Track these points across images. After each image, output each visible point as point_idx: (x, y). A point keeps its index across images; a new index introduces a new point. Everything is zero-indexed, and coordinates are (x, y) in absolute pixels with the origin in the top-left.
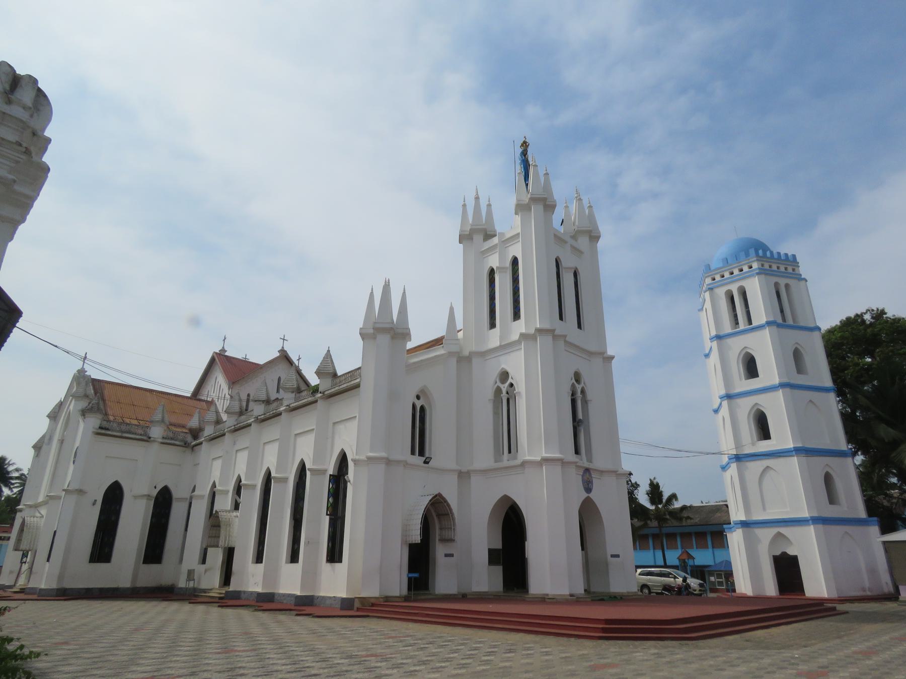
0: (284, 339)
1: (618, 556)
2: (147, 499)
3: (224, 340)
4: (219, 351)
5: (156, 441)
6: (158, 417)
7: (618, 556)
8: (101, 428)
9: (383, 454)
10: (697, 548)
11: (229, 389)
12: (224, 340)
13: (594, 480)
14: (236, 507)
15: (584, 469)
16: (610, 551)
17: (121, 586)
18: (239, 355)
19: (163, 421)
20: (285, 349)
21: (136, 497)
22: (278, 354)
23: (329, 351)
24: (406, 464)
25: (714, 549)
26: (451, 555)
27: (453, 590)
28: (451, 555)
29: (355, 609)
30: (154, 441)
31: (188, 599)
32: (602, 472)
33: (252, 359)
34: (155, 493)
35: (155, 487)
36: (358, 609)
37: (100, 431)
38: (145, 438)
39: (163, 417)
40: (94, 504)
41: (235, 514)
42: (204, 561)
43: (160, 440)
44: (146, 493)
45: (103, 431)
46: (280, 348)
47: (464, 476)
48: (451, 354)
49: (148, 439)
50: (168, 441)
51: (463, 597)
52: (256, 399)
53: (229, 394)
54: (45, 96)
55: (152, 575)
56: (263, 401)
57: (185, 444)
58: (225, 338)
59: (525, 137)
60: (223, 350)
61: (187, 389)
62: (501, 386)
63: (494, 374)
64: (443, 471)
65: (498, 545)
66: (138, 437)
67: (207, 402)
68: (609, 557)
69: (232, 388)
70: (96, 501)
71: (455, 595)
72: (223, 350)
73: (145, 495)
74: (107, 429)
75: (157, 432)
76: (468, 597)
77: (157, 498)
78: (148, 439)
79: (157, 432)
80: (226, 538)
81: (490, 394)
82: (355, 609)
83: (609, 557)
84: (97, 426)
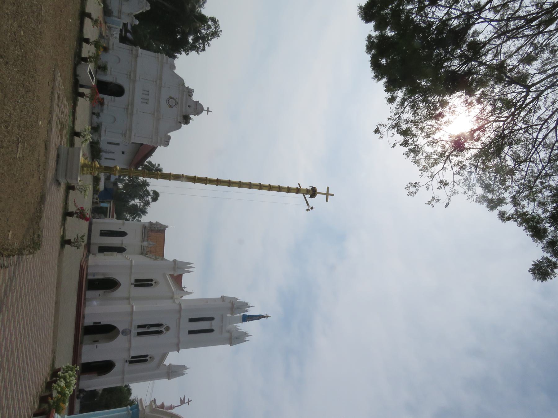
6: (151, 243)
8: (145, 227)
9: (133, 264)
13: (127, 336)
19: (149, 244)
21: (122, 241)
27: (87, 297)
34: (124, 246)
35: (126, 246)
37: (144, 227)
40: (120, 229)
43: (143, 245)
44: (124, 243)
48: (173, 293)
49: (143, 241)
55: (95, 249)
59: (270, 316)
65: (102, 324)
70: (121, 229)
74: (145, 229)
75: (145, 244)
77: (122, 248)
79: (145, 244)
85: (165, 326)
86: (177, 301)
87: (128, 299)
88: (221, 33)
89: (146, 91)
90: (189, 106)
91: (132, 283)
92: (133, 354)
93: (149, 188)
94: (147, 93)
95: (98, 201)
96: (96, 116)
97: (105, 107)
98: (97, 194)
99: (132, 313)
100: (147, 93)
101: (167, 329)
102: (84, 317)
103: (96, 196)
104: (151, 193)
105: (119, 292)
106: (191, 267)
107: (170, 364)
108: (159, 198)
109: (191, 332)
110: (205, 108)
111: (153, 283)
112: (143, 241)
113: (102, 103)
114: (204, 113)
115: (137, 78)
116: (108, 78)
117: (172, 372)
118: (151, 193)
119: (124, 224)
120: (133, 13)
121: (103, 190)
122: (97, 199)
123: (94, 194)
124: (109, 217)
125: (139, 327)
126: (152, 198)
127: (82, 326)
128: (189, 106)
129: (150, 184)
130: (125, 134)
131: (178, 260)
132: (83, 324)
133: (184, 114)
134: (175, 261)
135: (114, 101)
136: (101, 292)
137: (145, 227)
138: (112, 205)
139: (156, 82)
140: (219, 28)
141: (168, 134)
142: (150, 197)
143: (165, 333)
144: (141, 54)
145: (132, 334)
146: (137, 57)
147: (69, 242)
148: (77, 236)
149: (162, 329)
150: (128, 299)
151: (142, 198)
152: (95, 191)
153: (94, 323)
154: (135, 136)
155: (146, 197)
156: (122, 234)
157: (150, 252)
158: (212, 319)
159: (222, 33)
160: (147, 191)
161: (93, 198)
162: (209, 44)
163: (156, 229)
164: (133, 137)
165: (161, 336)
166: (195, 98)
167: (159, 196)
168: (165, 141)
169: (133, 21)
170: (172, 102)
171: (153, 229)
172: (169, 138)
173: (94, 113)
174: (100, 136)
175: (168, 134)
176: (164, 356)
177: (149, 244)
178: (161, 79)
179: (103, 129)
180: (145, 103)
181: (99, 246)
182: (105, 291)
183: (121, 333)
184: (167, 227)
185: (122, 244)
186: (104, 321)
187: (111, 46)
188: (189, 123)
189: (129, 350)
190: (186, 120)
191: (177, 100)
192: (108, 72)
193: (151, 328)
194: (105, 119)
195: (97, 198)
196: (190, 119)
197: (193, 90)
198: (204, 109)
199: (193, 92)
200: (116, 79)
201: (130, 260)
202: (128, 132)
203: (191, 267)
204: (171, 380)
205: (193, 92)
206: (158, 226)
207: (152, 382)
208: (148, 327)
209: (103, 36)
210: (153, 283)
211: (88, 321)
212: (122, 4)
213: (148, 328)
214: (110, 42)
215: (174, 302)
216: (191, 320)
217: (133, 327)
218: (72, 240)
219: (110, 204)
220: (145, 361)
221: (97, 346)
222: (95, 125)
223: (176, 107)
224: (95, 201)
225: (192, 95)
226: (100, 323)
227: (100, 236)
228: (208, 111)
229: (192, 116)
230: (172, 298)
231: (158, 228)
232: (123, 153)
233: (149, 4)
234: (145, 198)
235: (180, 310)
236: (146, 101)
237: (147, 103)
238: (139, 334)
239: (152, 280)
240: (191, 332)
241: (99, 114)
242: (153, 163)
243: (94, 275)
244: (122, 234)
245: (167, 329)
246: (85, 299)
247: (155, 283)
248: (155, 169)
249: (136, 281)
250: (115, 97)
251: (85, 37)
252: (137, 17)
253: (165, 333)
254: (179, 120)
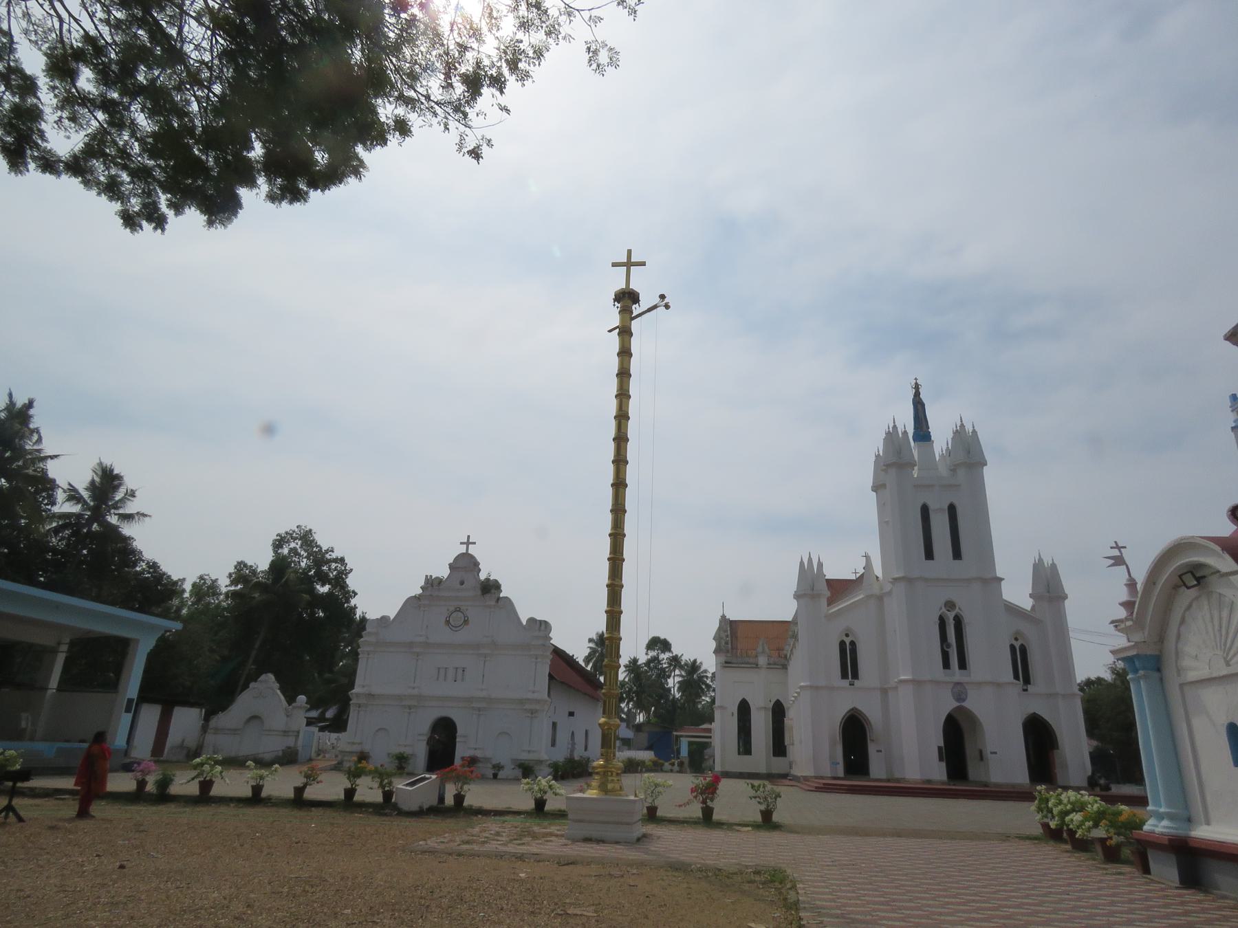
8: (726, 662)
9: (808, 684)
17: (761, 772)
19: (763, 652)
21: (759, 709)
26: (881, 751)
27: (884, 777)
28: (881, 751)
30: (761, 667)
35: (770, 701)
38: (754, 666)
39: (763, 650)
43: (765, 666)
45: (727, 665)
48: (869, 597)
49: (757, 666)
55: (778, 765)
59: (916, 379)
65: (942, 744)
73: (762, 708)
74: (730, 663)
75: (762, 661)
78: (757, 666)
79: (762, 661)
85: (944, 609)
86: (888, 587)
87: (884, 691)
88: (303, 527)
89: (439, 672)
90: (462, 583)
91: (850, 685)
92: (1009, 676)
93: (642, 659)
94: (442, 672)
95: (676, 762)
96: (499, 770)
97: (479, 754)
98: (663, 765)
99: (916, 683)
100: (442, 672)
101: (950, 605)
102: (929, 782)
103: (667, 765)
104: (652, 654)
105: (872, 712)
106: (810, 560)
107: (1031, 596)
108: (662, 637)
109: (957, 554)
110: (463, 549)
111: (848, 640)
112: (757, 665)
113: (472, 761)
114: (472, 550)
115: (415, 692)
116: (420, 752)
117: (1049, 592)
118: (652, 654)
119: (722, 707)
120: (284, 707)
121: (653, 753)
122: (673, 764)
123: (662, 771)
124: (710, 737)
125: (946, 665)
126: (663, 652)
127: (950, 785)
128: (462, 583)
129: (632, 658)
130: (533, 712)
131: (795, 590)
132: (943, 783)
133: (479, 593)
134: (797, 596)
135: (465, 736)
136: (872, 749)
137: (726, 662)
138: (685, 732)
139: (418, 654)
140: (294, 531)
141: (524, 623)
142: (662, 656)
143: (959, 611)
144: (363, 687)
145: (964, 679)
146: (371, 696)
147: (767, 815)
148: (753, 799)
149: (950, 616)
150: (884, 691)
151: (665, 672)
152: (656, 767)
153: (941, 759)
154: (533, 692)
155: (662, 664)
156: (744, 709)
157: (779, 649)
158: (925, 511)
159: (303, 524)
160: (648, 663)
161: (672, 771)
162: (328, 550)
163: (729, 639)
164: (536, 696)
165: (967, 619)
166: (444, 572)
167: (659, 638)
168: (540, 630)
169: (300, 707)
170: (457, 618)
171: (730, 646)
172: (532, 621)
173: (495, 776)
174: (540, 762)
175: (524, 623)
176: (1013, 610)
177: (763, 652)
178: (411, 645)
179: (524, 756)
180: (463, 675)
181: (772, 755)
182: (869, 741)
183: (963, 704)
184: (723, 617)
186: (936, 739)
187: (357, 748)
188: (496, 581)
189: (999, 685)
190: (490, 588)
191: (452, 609)
192: (407, 751)
193: (949, 641)
194: (504, 754)
195: (670, 764)
196: (487, 580)
197: (427, 576)
198: (465, 552)
199: (431, 576)
200: (420, 735)
201: (798, 690)
202: (527, 706)
203: (810, 560)
204: (1066, 592)
205: (431, 576)
206: (723, 635)
207: (1071, 634)
208: (947, 648)
209: (338, 763)
210: (850, 641)
211: (938, 772)
212: (270, 730)
213: (949, 646)
214: (348, 750)
215: (890, 593)
216: (929, 555)
217: (948, 679)
218: (763, 807)
219: (681, 736)
220: (1024, 650)
221: (992, 753)
222: (518, 772)
223: (467, 610)
224: (676, 768)
225: (437, 578)
226: (940, 748)
227: (751, 755)
228: (468, 543)
229: (483, 576)
230: (880, 598)
231: (727, 636)
232: (571, 714)
233: (263, 677)
234: (665, 666)
235: (908, 580)
236: (460, 672)
237: (463, 671)
238: (963, 665)
239: (842, 644)
240: (957, 554)
241: (494, 767)
242: (587, 652)
243: (834, 764)
244: (744, 709)
245: (950, 605)
246: (888, 781)
247: (847, 635)
248: (599, 649)
249: (844, 675)
250: (457, 734)
251: (342, 797)
252: (291, 700)
253: (959, 608)
254: (493, 603)
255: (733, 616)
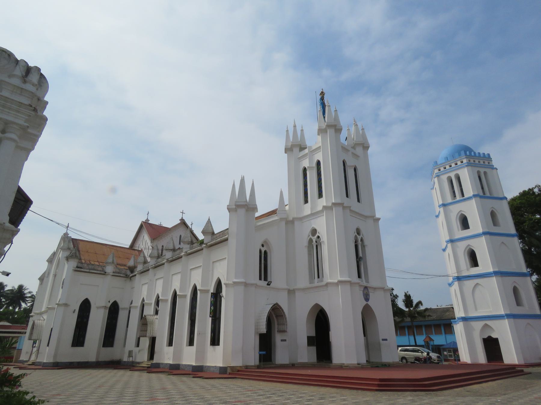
0: (183, 213)
1: (386, 340)
2: (105, 309)
3: (148, 214)
4: (145, 221)
5: (109, 274)
6: (110, 260)
7: (386, 340)
8: (77, 267)
10: (400, 335)
11: (151, 243)
12: (148, 214)
13: (371, 294)
14: (157, 313)
15: (364, 287)
16: (381, 338)
17: (90, 360)
18: (157, 223)
19: (113, 262)
20: (184, 218)
21: (98, 308)
22: (179, 222)
23: (209, 219)
24: (256, 286)
25: (409, 336)
26: (285, 340)
27: (286, 361)
28: (285, 340)
29: (228, 373)
30: (108, 274)
31: (129, 368)
32: (375, 289)
33: (164, 225)
34: (109, 305)
35: (109, 302)
36: (230, 374)
37: (77, 269)
39: (113, 260)
40: (74, 312)
41: (156, 317)
42: (138, 345)
43: (112, 274)
45: (79, 269)
46: (181, 218)
47: (291, 292)
48: (281, 219)
49: (105, 273)
50: (116, 274)
51: (293, 366)
52: (167, 249)
53: (151, 246)
54: (45, 78)
55: (108, 354)
56: (171, 250)
57: (126, 276)
58: (148, 213)
59: (322, 89)
60: (147, 220)
61: (126, 243)
62: (313, 238)
63: (308, 231)
64: (278, 289)
65: (313, 334)
66: (98, 272)
67: (138, 251)
68: (381, 340)
69: (153, 242)
70: (75, 310)
71: (288, 364)
72: (147, 220)
73: (103, 307)
74: (81, 268)
75: (109, 269)
76: (296, 365)
77: (110, 308)
78: (105, 273)
79: (109, 269)
80: (151, 332)
81: (306, 243)
82: (228, 373)
83: (381, 340)
84: (75, 266)
181: (102, 345)
185: (105, 307)
255: (73, 235)
